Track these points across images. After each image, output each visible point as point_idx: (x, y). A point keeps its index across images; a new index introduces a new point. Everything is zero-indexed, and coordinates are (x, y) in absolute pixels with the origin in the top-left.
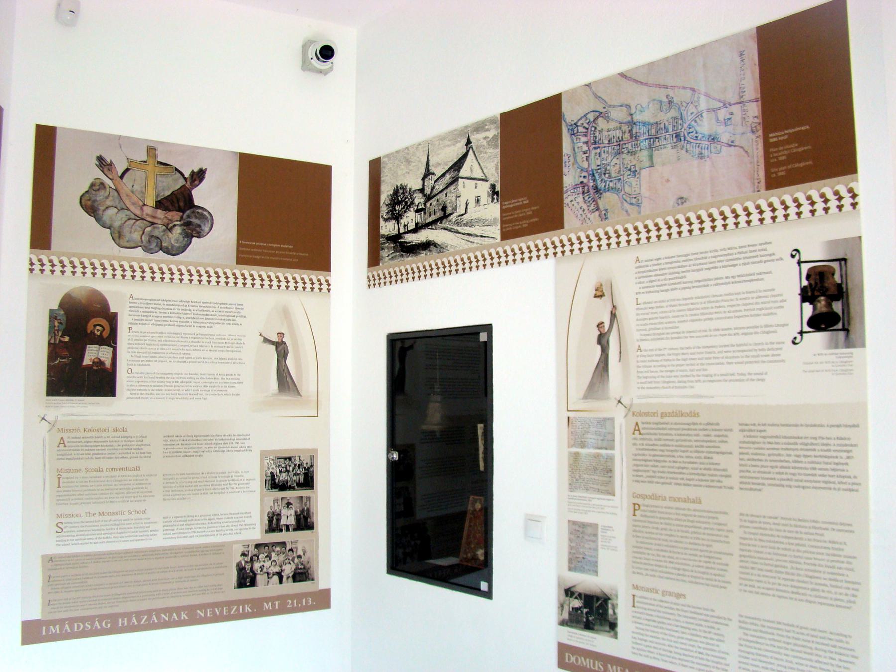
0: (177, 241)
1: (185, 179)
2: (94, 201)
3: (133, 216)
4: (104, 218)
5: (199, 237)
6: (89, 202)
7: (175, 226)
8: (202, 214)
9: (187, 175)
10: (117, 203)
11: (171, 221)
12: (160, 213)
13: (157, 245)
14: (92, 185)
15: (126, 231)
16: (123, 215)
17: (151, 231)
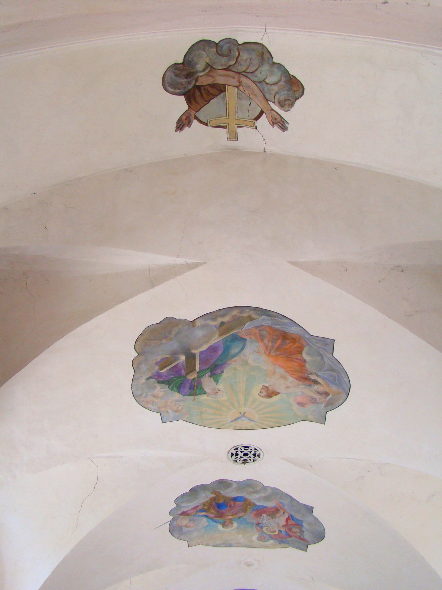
0: (200, 56)
1: (196, 118)
2: (289, 90)
3: (249, 75)
4: (279, 74)
5: (176, 64)
6: (295, 88)
7: (204, 70)
8: (175, 88)
9: (195, 122)
10: (266, 88)
11: (208, 75)
12: (220, 80)
13: (222, 47)
14: (292, 105)
15: (256, 61)
16: (260, 76)
17: (229, 60)
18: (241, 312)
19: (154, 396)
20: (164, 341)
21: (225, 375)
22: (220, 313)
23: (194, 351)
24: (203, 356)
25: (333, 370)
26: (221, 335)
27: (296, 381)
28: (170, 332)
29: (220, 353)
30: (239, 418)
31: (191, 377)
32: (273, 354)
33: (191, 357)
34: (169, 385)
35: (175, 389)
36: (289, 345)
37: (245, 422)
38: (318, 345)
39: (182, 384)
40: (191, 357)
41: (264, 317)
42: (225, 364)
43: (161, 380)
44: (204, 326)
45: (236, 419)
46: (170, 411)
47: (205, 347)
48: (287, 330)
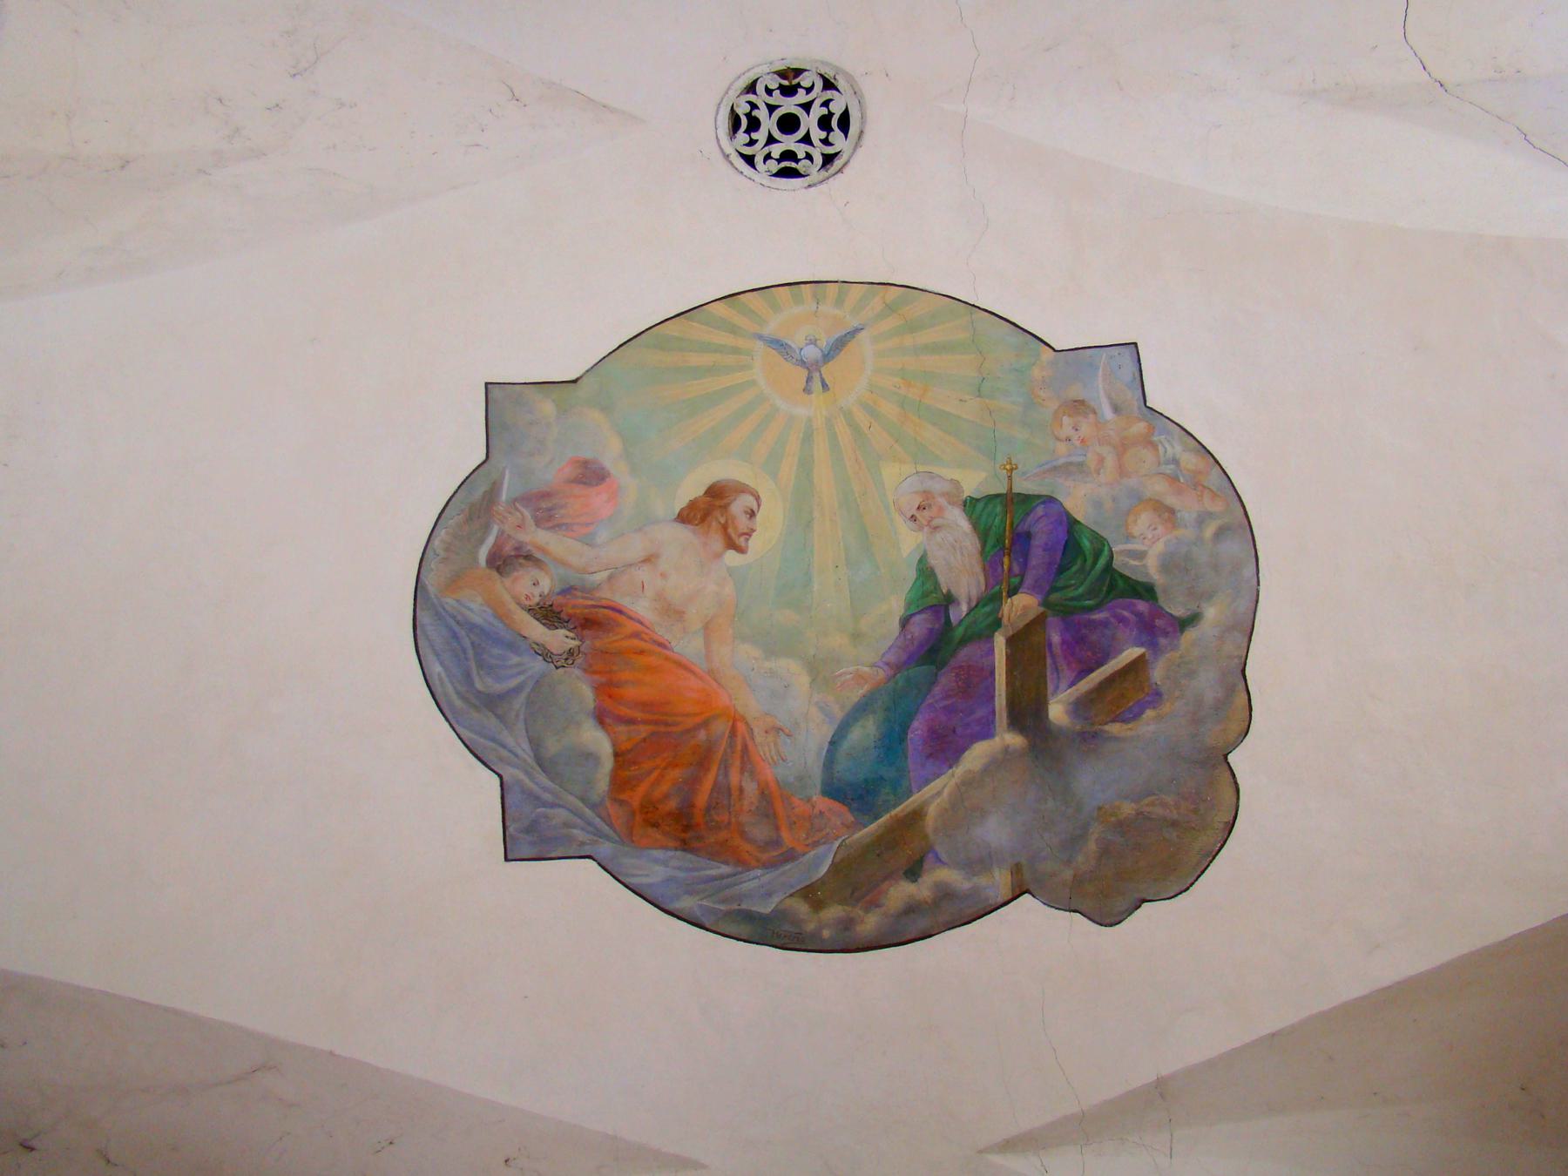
18: (847, 924)
19: (1167, 514)
20: (1128, 809)
21: (895, 606)
22: (922, 923)
23: (1014, 740)
24: (980, 713)
25: (492, 702)
26: (917, 815)
27: (624, 602)
28: (1105, 851)
29: (918, 727)
30: (827, 357)
31: (1021, 606)
32: (720, 728)
33: (1027, 713)
34: (1109, 567)
35: (1086, 543)
36: (664, 787)
37: (806, 328)
38: (561, 815)
39: (1062, 570)
40: (1027, 713)
41: (766, 908)
42: (898, 668)
43: (1142, 606)
44: (978, 864)
45: (840, 344)
46: (1108, 413)
47: (977, 755)
48: (679, 858)
